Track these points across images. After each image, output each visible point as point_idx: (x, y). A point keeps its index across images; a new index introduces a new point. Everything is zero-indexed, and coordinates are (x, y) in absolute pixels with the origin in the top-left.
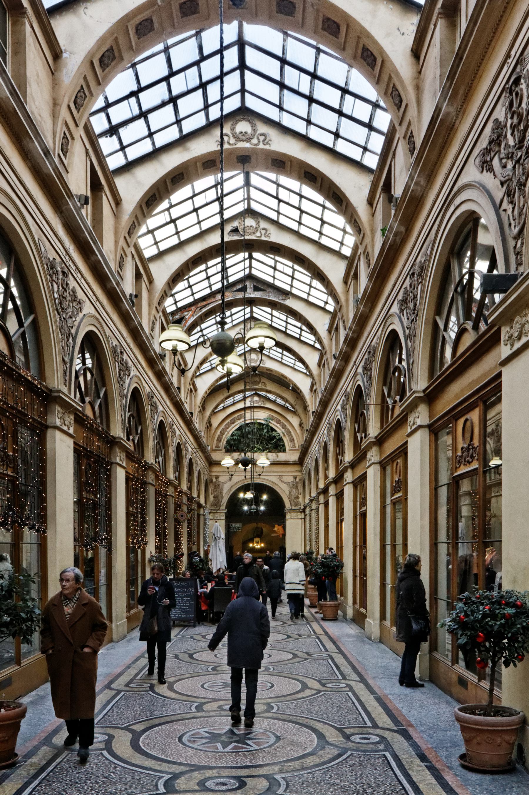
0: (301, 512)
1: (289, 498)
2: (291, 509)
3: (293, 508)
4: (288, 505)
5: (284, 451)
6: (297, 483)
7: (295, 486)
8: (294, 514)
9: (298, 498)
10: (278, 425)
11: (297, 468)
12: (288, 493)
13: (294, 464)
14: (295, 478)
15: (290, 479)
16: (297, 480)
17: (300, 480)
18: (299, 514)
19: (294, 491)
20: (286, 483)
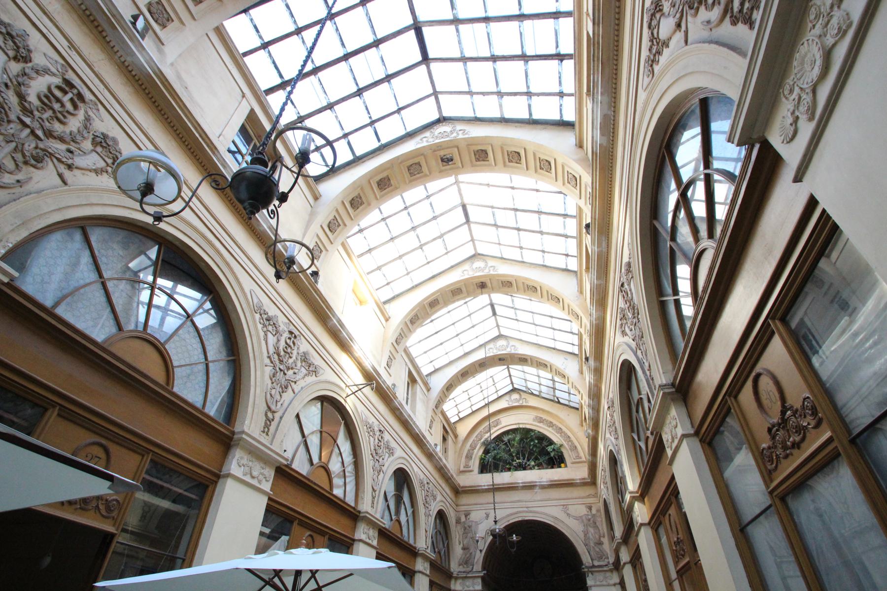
0: (611, 571)
1: (586, 545)
2: (594, 566)
3: (596, 563)
4: (586, 559)
5: (566, 466)
6: (594, 516)
7: (590, 522)
8: (600, 576)
9: (600, 543)
10: (550, 429)
11: (589, 490)
12: (582, 535)
13: (584, 484)
14: (590, 508)
15: (582, 511)
16: (594, 511)
17: (598, 511)
18: (608, 574)
19: (591, 530)
20: (576, 518)
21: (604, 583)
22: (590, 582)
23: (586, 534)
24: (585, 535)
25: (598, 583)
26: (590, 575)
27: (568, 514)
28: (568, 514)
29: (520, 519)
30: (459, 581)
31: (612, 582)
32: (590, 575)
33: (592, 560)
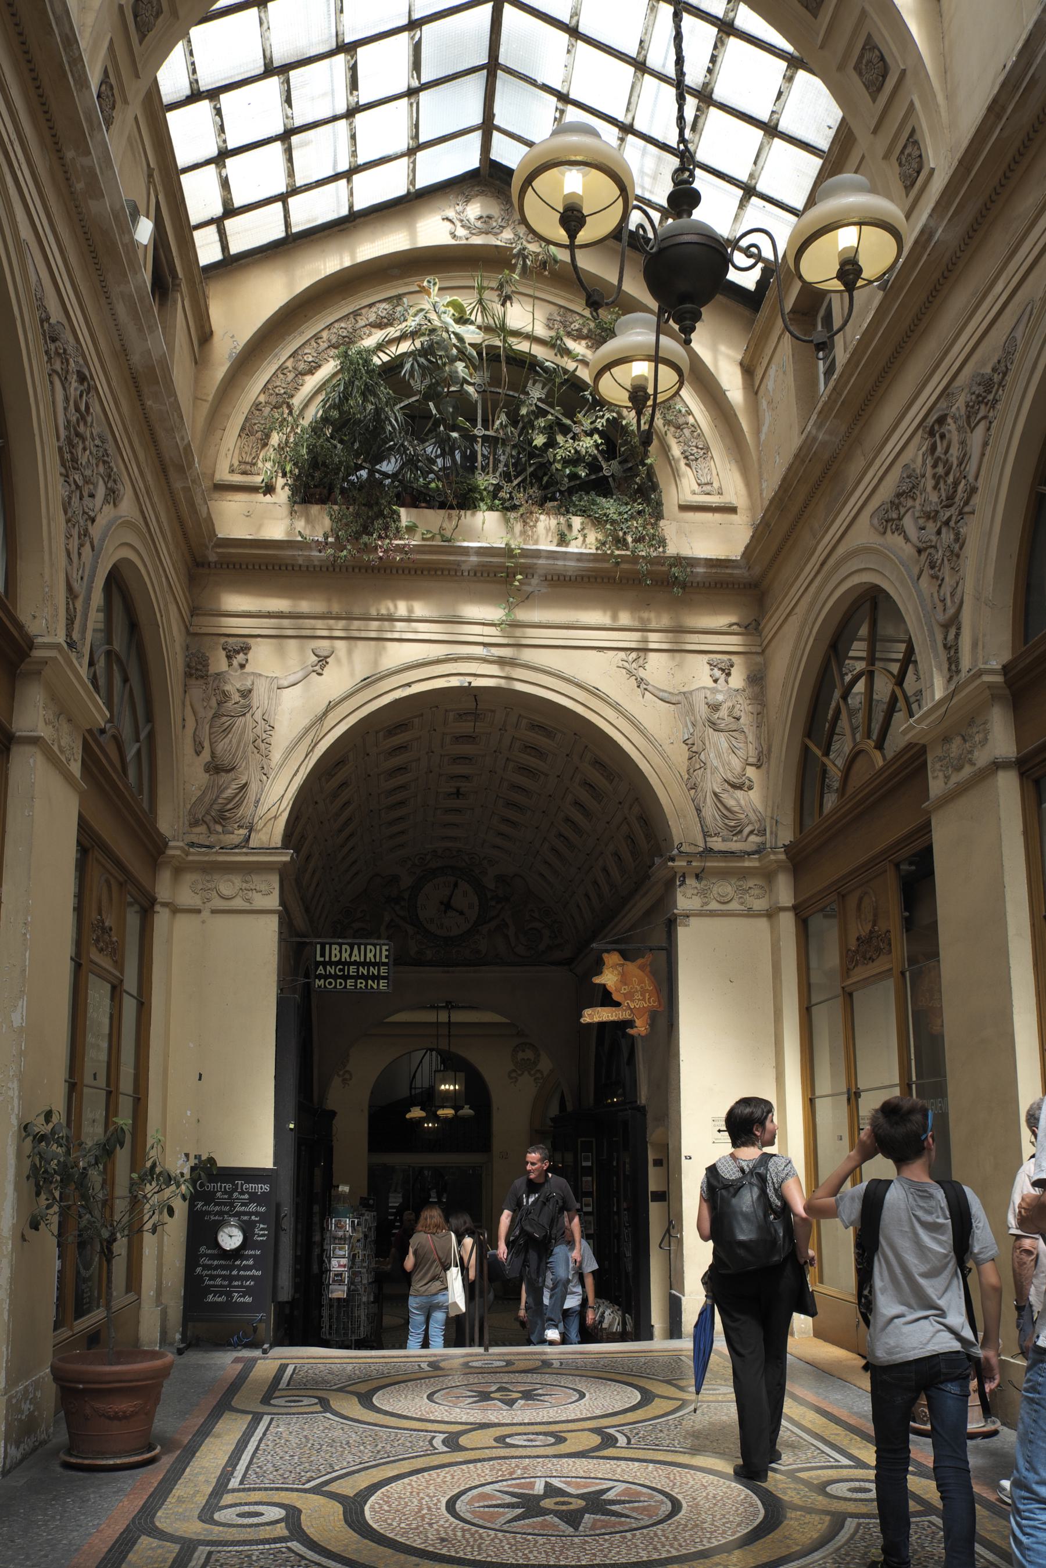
2: (708, 852)
4: (683, 827)
12: (679, 755)
21: (734, 906)
22: (685, 900)
23: (694, 752)
24: (694, 755)
25: (714, 906)
26: (691, 882)
27: (640, 682)
28: (640, 682)
29: (455, 682)
30: (189, 878)
31: (760, 904)
32: (691, 882)
33: (706, 834)
